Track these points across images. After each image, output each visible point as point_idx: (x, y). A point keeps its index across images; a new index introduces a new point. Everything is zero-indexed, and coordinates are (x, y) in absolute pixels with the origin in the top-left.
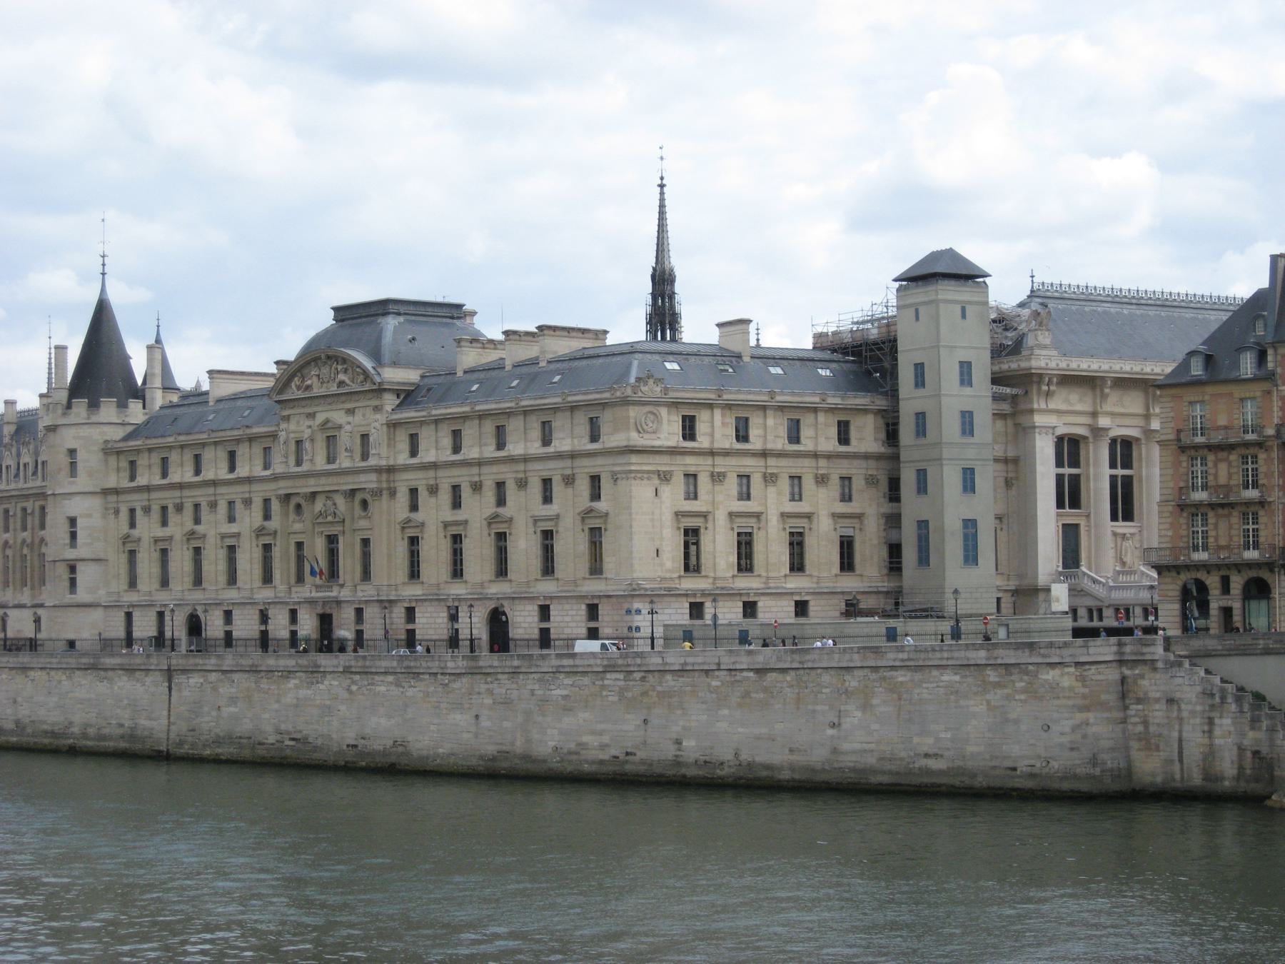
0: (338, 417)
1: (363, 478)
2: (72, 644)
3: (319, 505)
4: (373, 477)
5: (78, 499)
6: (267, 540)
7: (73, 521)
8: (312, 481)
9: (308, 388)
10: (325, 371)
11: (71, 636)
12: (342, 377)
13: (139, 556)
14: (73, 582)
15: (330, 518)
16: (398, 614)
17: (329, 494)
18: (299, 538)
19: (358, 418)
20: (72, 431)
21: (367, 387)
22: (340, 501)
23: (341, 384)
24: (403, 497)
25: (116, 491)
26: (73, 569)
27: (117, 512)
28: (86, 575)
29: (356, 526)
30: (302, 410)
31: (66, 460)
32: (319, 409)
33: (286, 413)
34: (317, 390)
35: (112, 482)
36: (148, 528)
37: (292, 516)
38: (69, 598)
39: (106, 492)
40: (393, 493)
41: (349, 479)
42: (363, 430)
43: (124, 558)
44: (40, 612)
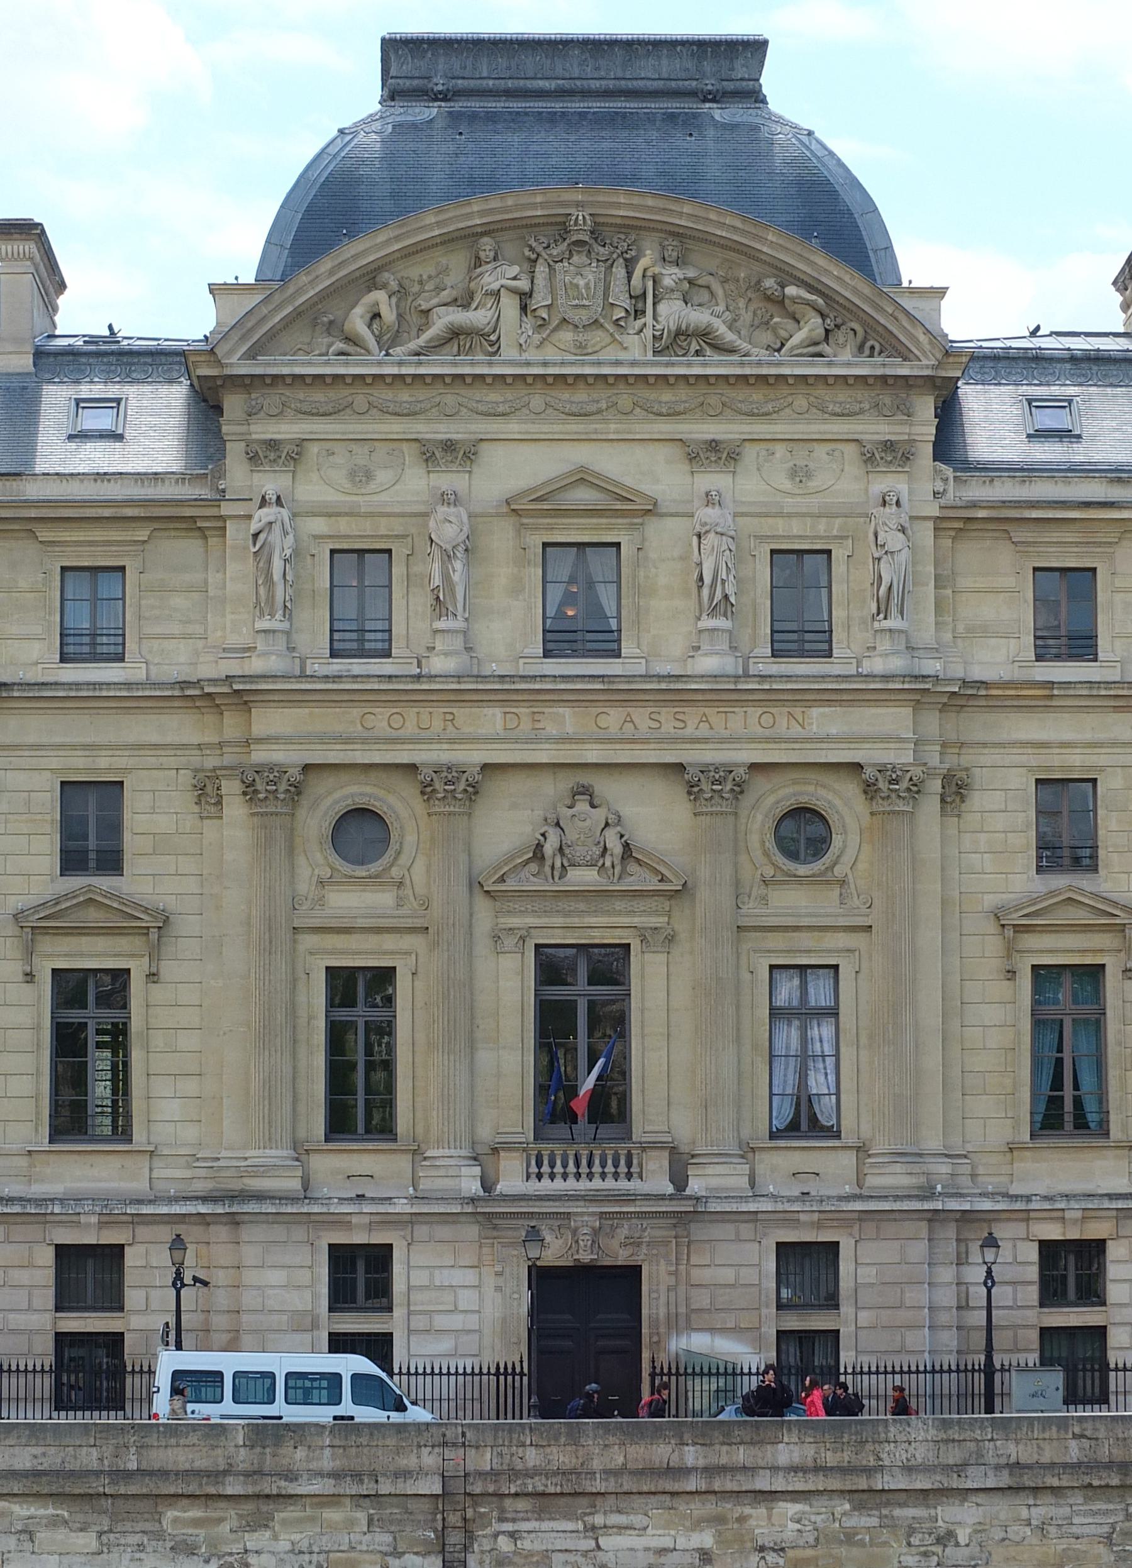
0: (642, 463)
1: (822, 720)
3: (505, 826)
4: (895, 719)
6: (93, 955)
8: (492, 720)
9: (486, 339)
10: (582, 275)
12: (672, 313)
15: (584, 877)
16: (1020, 1261)
17: (582, 783)
18: (361, 954)
19: (754, 484)
21: (845, 361)
22: (657, 818)
23: (679, 339)
24: (1004, 814)
29: (753, 913)
30: (396, 428)
32: (513, 428)
33: (286, 430)
34: (519, 349)
37: (316, 859)
40: (956, 790)
41: (746, 720)
42: (797, 533)
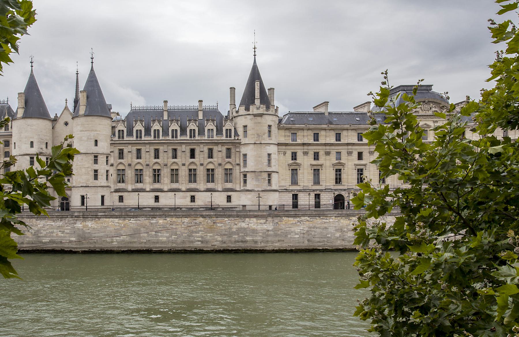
2: (270, 207)
5: (272, 146)
7: (269, 155)
11: (271, 204)
13: (300, 172)
14: (269, 181)
20: (271, 117)
25: (286, 145)
26: (269, 175)
27: (285, 154)
28: (275, 177)
31: (266, 129)
35: (282, 140)
36: (306, 162)
38: (269, 188)
39: (279, 144)
43: (289, 173)
44: (229, 193)
